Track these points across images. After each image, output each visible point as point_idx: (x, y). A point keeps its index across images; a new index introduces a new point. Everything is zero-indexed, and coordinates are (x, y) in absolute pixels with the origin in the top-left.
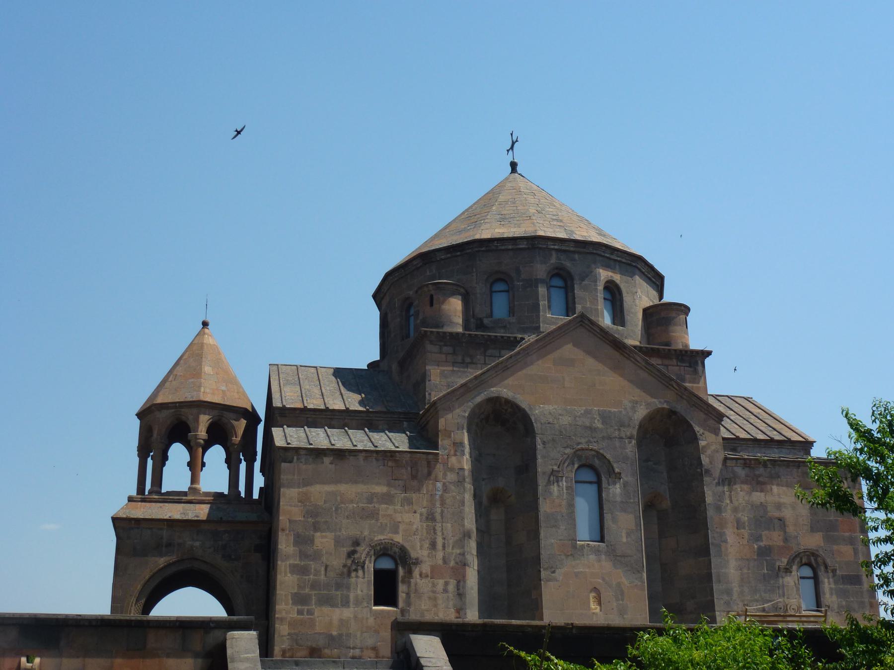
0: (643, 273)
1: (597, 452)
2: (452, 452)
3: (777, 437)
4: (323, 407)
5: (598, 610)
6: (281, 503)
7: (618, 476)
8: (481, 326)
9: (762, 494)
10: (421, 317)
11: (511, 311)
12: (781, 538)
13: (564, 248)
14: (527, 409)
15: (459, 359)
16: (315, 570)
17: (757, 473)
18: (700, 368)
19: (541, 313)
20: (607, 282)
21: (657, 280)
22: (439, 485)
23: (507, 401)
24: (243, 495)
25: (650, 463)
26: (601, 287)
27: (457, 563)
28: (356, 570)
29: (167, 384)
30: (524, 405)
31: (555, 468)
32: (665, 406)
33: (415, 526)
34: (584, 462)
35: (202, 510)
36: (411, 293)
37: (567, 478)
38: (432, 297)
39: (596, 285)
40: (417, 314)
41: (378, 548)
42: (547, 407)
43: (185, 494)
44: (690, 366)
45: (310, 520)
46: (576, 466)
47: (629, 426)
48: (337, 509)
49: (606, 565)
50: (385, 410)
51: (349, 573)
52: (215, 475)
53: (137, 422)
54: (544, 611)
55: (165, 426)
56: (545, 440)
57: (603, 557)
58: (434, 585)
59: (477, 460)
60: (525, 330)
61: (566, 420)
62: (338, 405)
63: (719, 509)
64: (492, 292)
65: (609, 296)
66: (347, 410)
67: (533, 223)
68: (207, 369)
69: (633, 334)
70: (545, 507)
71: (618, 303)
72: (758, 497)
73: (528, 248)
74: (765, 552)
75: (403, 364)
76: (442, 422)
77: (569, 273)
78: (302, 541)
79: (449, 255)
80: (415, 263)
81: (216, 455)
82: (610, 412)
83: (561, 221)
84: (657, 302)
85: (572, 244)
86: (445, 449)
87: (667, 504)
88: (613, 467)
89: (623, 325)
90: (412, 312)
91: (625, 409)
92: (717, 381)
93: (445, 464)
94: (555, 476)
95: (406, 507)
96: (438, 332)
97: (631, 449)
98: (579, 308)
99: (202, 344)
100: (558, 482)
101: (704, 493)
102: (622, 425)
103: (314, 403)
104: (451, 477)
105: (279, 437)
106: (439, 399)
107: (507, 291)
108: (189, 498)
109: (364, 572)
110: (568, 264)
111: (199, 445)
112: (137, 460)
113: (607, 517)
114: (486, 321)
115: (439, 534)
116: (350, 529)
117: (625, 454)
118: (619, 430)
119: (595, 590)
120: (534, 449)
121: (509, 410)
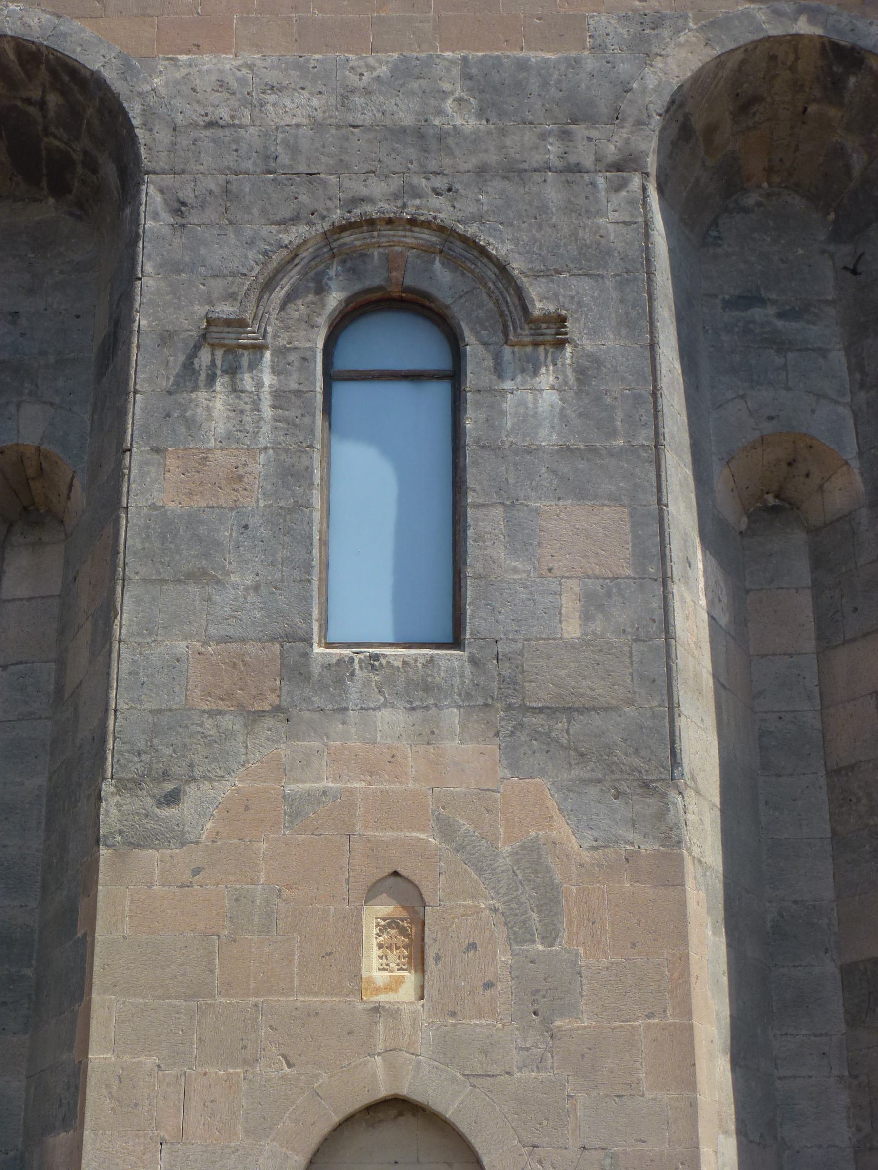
1: (442, 229)
5: (407, 992)
7: (553, 332)
14: (110, 75)
25: (757, 313)
32: (803, 27)
34: (374, 278)
37: (281, 352)
42: (207, 60)
47: (616, 117)
49: (467, 755)
54: (96, 997)
56: (186, 194)
57: (452, 716)
61: (296, 108)
70: (152, 487)
82: (522, 65)
88: (520, 294)
91: (599, 48)
94: (225, 345)
100: (233, 371)
113: (486, 522)
118: (565, 135)
119: (397, 882)
121: (53, 99)
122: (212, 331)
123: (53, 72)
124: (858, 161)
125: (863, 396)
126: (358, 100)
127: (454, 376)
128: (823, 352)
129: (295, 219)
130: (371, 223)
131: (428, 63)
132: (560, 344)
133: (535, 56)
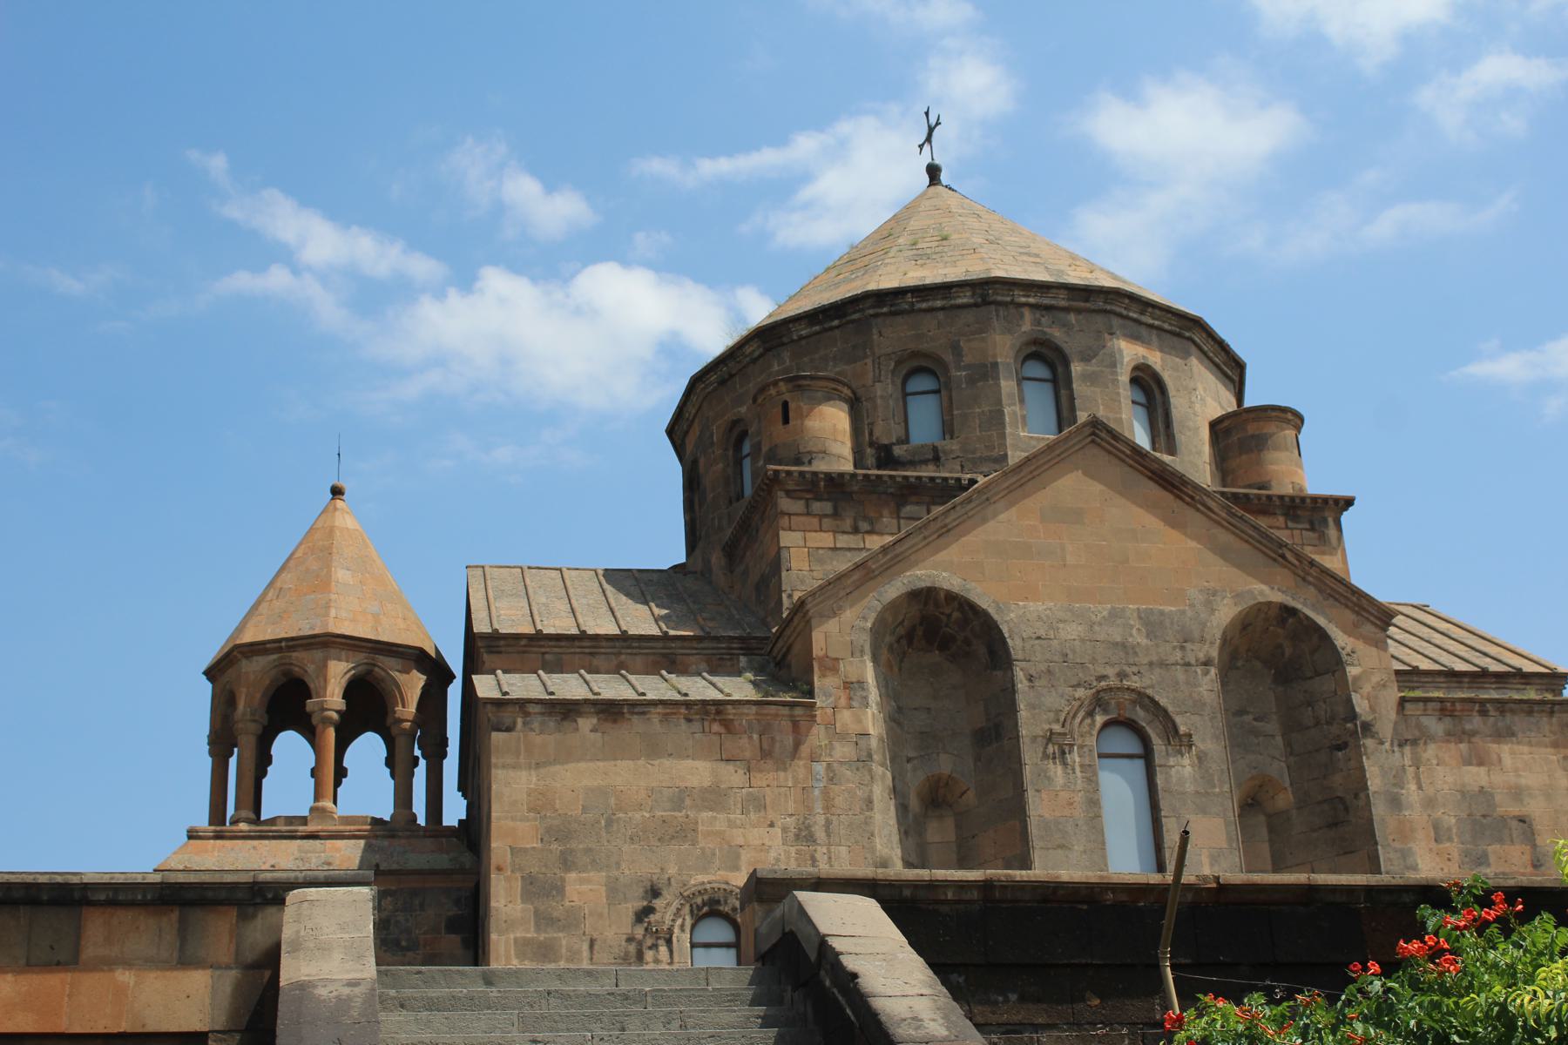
0: (1205, 353)
2: (843, 702)
3: (1494, 667)
4: (575, 631)
6: (494, 815)
9: (1482, 770)
10: (765, 449)
11: (948, 430)
12: (1527, 857)
13: (1046, 301)
14: (991, 611)
15: (848, 524)
16: (569, 950)
17: (1468, 727)
18: (1332, 532)
19: (1008, 430)
20: (1137, 368)
21: (1232, 369)
22: (820, 768)
23: (951, 597)
24: (421, 821)
25: (1248, 718)
26: (1124, 378)
28: (654, 947)
29: (264, 608)
30: (984, 603)
31: (1057, 728)
33: (773, 854)
35: (338, 850)
36: (743, 409)
37: (1081, 747)
38: (785, 405)
39: (1115, 373)
40: (757, 448)
41: (699, 900)
42: (1032, 606)
43: (303, 820)
44: (1312, 529)
45: (554, 846)
46: (1100, 719)
47: (1202, 640)
48: (609, 823)
50: (699, 633)
51: (640, 957)
52: (368, 782)
53: (208, 687)
55: (264, 696)
56: (1033, 672)
59: (896, 717)
60: (975, 463)
62: (608, 628)
63: (1396, 802)
64: (905, 395)
65: (1141, 398)
66: (624, 638)
67: (982, 259)
68: (341, 575)
69: (1196, 459)
70: (1039, 807)
71: (1160, 411)
72: (1476, 776)
73: (976, 305)
75: (732, 552)
76: (818, 637)
77: (1058, 350)
78: (539, 889)
79: (817, 328)
80: (748, 349)
81: (368, 750)
82: (1162, 613)
83: (1037, 256)
84: (1232, 407)
85: (1063, 294)
86: (827, 695)
87: (1284, 800)
89: (1172, 451)
90: (746, 448)
91: (1192, 606)
92: (1369, 557)
94: (1058, 746)
95: (752, 816)
96: (802, 474)
97: (1208, 685)
98: (1082, 417)
99: (331, 530)
101: (1362, 769)
102: (1186, 639)
103: (558, 623)
104: (843, 751)
105: (485, 686)
106: (813, 594)
107: (937, 392)
108: (311, 828)
109: (671, 952)
110: (1057, 334)
111: (327, 721)
112: (207, 762)
114: (898, 451)
116: (639, 865)
117: (1196, 697)
118: (1182, 648)
120: (1012, 690)
121: (956, 615)
122: (1050, 737)
123: (961, 605)
124: (1288, 652)
125: (1292, 759)
126: (1097, 628)
127: (1147, 755)
128: (1273, 736)
129: (1079, 685)
130: (1111, 689)
131: (1123, 610)
132: (1190, 746)
133: (1167, 609)
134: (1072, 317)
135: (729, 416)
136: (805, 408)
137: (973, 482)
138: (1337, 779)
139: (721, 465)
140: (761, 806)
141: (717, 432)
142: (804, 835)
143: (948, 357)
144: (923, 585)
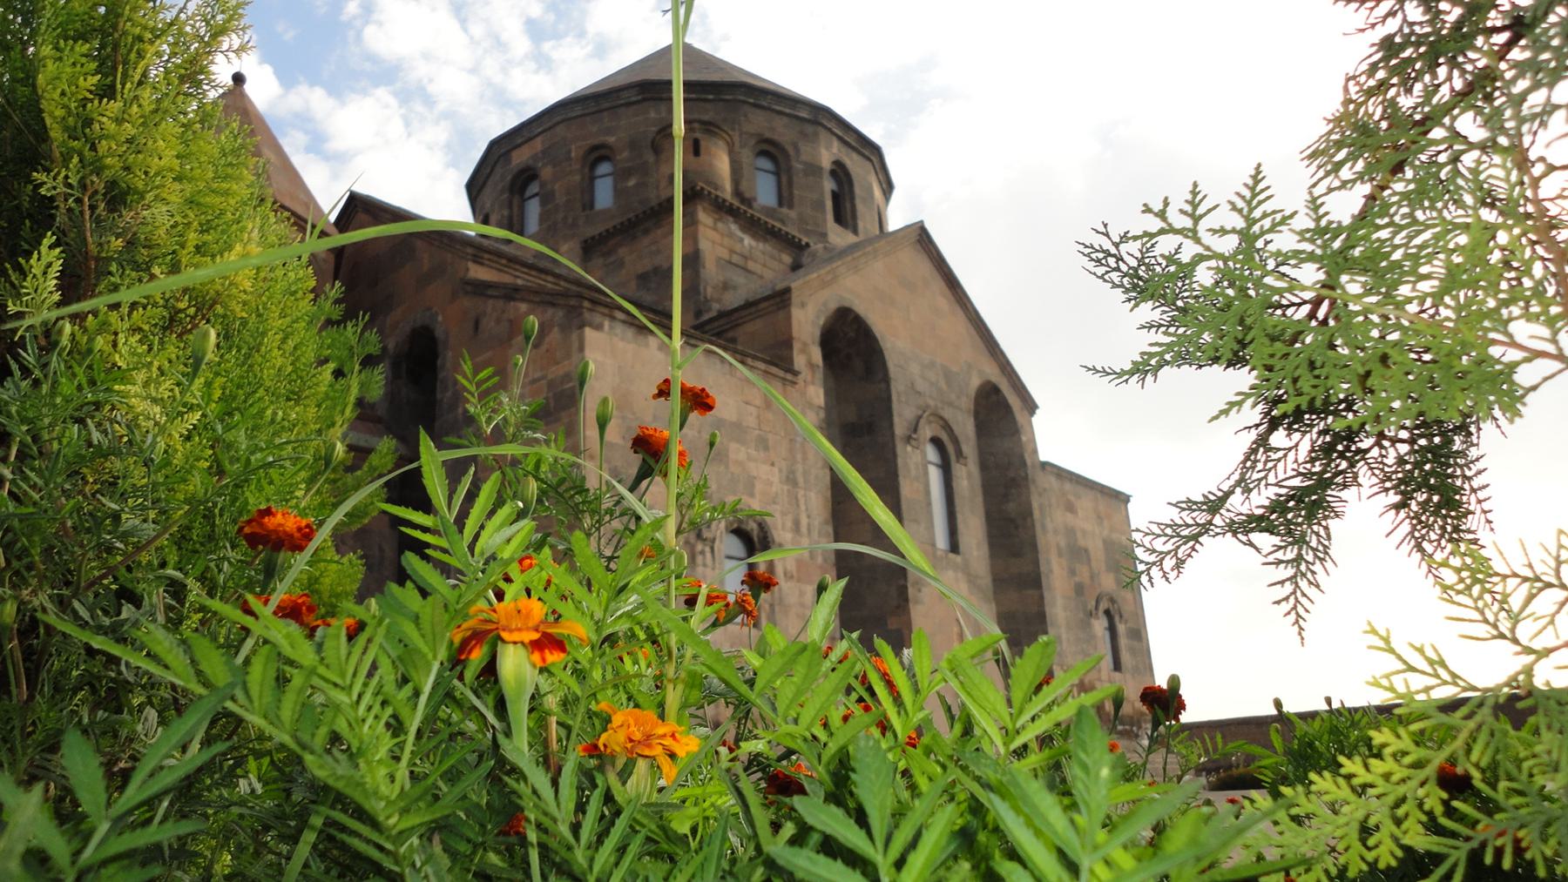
2: (809, 378)
8: (750, 206)
27: (825, 560)
28: (702, 553)
57: (960, 575)
58: (802, 594)
60: (807, 233)
61: (915, 369)
63: (1043, 526)
74: (1079, 589)
80: (625, 94)
90: (604, 168)
93: (803, 394)
114: (755, 205)
115: (803, 507)
121: (852, 334)
134: (855, 156)
135: (596, 141)
136: (713, 149)
137: (808, 245)
138: (1011, 507)
139: (577, 178)
140: (766, 448)
141: (576, 152)
142: (790, 480)
143: (791, 151)
144: (847, 304)
